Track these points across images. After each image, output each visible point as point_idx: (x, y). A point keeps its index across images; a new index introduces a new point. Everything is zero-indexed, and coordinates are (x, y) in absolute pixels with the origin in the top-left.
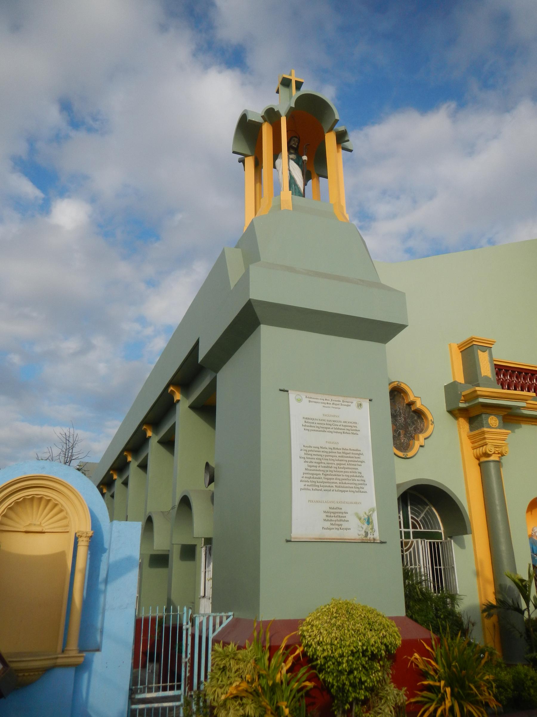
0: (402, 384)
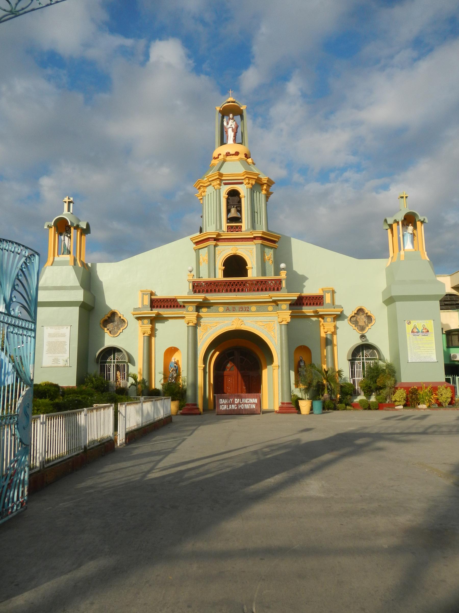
0: (116, 310)
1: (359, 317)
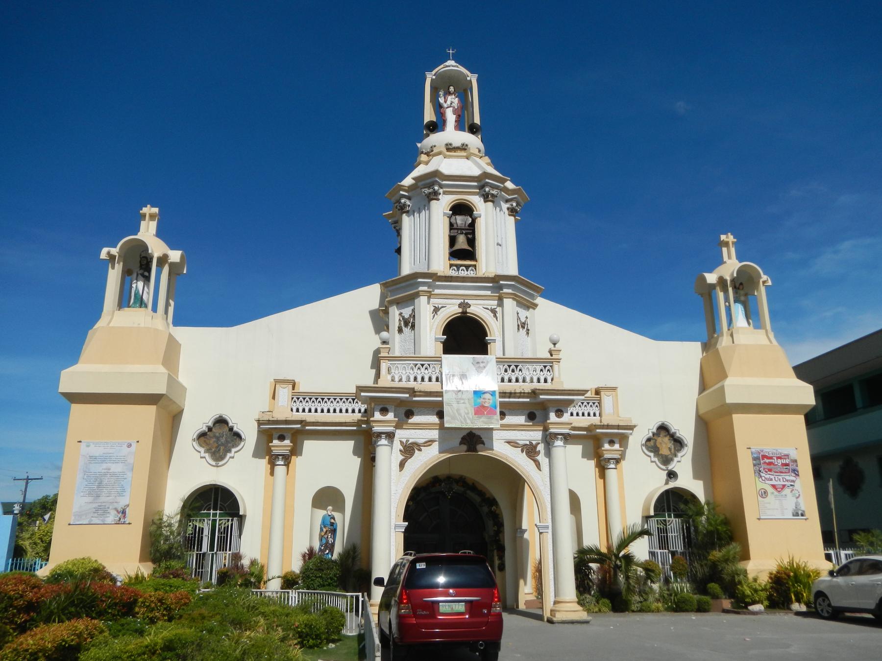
0: (224, 416)
1: (659, 440)
